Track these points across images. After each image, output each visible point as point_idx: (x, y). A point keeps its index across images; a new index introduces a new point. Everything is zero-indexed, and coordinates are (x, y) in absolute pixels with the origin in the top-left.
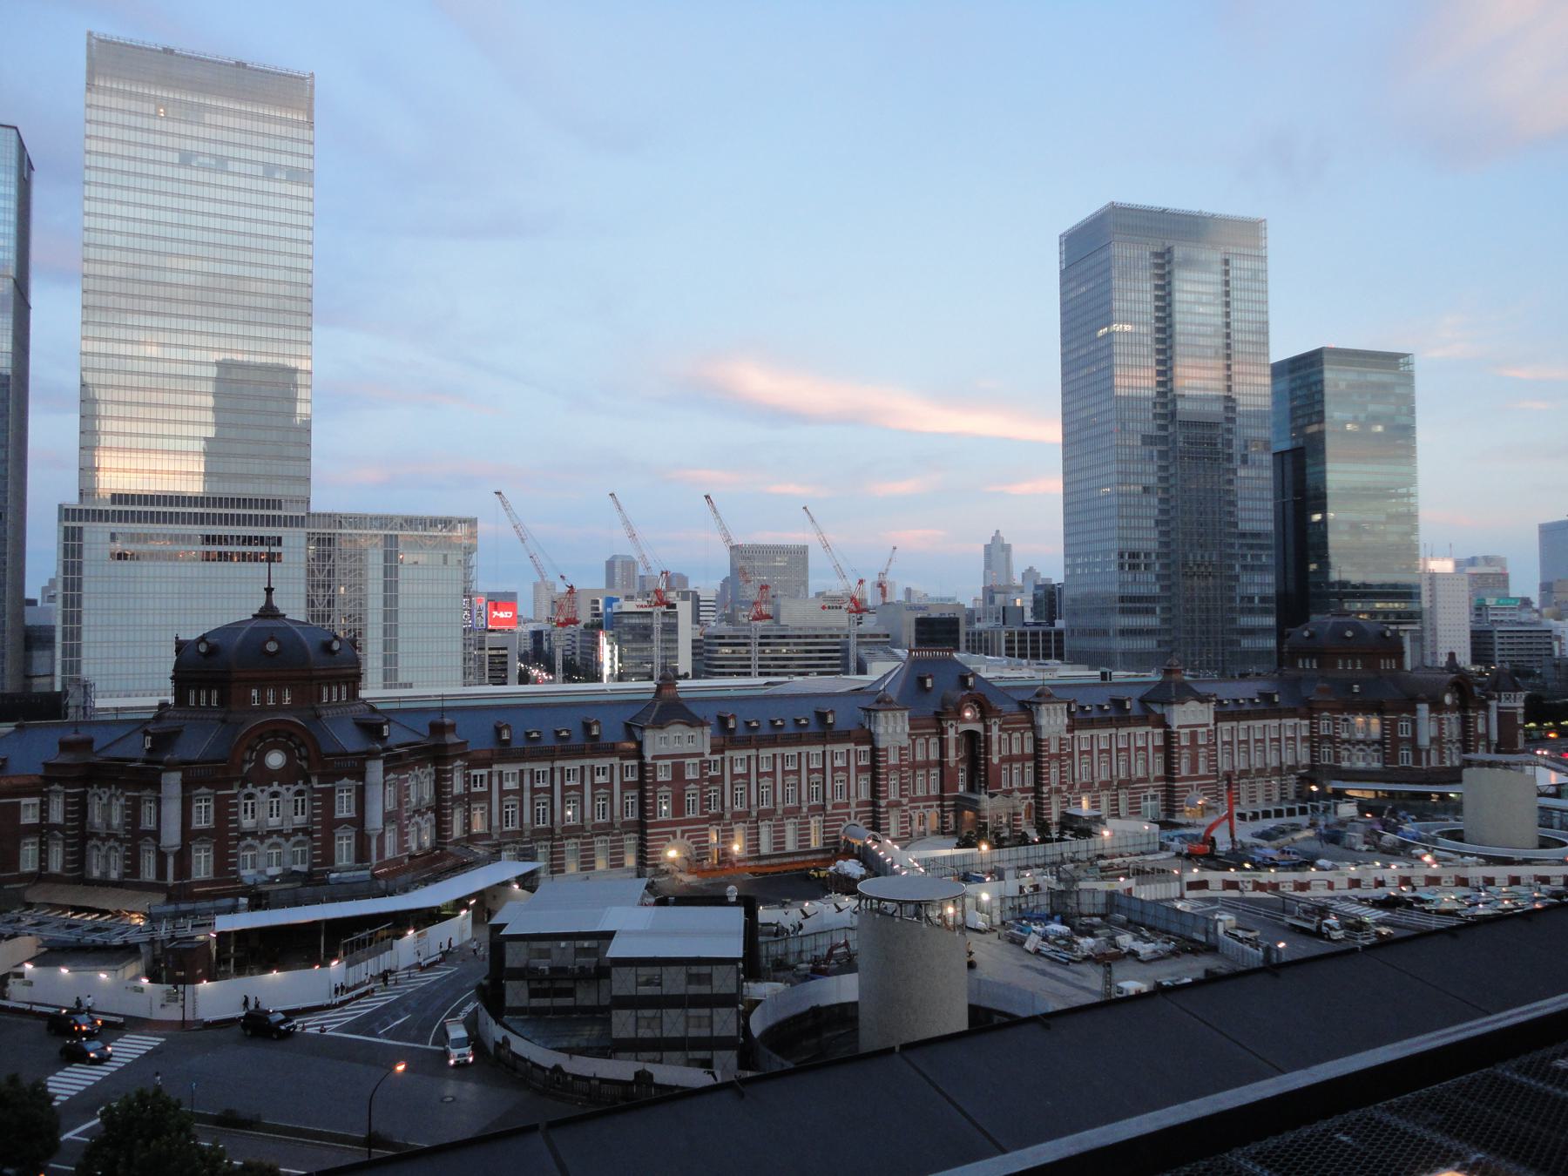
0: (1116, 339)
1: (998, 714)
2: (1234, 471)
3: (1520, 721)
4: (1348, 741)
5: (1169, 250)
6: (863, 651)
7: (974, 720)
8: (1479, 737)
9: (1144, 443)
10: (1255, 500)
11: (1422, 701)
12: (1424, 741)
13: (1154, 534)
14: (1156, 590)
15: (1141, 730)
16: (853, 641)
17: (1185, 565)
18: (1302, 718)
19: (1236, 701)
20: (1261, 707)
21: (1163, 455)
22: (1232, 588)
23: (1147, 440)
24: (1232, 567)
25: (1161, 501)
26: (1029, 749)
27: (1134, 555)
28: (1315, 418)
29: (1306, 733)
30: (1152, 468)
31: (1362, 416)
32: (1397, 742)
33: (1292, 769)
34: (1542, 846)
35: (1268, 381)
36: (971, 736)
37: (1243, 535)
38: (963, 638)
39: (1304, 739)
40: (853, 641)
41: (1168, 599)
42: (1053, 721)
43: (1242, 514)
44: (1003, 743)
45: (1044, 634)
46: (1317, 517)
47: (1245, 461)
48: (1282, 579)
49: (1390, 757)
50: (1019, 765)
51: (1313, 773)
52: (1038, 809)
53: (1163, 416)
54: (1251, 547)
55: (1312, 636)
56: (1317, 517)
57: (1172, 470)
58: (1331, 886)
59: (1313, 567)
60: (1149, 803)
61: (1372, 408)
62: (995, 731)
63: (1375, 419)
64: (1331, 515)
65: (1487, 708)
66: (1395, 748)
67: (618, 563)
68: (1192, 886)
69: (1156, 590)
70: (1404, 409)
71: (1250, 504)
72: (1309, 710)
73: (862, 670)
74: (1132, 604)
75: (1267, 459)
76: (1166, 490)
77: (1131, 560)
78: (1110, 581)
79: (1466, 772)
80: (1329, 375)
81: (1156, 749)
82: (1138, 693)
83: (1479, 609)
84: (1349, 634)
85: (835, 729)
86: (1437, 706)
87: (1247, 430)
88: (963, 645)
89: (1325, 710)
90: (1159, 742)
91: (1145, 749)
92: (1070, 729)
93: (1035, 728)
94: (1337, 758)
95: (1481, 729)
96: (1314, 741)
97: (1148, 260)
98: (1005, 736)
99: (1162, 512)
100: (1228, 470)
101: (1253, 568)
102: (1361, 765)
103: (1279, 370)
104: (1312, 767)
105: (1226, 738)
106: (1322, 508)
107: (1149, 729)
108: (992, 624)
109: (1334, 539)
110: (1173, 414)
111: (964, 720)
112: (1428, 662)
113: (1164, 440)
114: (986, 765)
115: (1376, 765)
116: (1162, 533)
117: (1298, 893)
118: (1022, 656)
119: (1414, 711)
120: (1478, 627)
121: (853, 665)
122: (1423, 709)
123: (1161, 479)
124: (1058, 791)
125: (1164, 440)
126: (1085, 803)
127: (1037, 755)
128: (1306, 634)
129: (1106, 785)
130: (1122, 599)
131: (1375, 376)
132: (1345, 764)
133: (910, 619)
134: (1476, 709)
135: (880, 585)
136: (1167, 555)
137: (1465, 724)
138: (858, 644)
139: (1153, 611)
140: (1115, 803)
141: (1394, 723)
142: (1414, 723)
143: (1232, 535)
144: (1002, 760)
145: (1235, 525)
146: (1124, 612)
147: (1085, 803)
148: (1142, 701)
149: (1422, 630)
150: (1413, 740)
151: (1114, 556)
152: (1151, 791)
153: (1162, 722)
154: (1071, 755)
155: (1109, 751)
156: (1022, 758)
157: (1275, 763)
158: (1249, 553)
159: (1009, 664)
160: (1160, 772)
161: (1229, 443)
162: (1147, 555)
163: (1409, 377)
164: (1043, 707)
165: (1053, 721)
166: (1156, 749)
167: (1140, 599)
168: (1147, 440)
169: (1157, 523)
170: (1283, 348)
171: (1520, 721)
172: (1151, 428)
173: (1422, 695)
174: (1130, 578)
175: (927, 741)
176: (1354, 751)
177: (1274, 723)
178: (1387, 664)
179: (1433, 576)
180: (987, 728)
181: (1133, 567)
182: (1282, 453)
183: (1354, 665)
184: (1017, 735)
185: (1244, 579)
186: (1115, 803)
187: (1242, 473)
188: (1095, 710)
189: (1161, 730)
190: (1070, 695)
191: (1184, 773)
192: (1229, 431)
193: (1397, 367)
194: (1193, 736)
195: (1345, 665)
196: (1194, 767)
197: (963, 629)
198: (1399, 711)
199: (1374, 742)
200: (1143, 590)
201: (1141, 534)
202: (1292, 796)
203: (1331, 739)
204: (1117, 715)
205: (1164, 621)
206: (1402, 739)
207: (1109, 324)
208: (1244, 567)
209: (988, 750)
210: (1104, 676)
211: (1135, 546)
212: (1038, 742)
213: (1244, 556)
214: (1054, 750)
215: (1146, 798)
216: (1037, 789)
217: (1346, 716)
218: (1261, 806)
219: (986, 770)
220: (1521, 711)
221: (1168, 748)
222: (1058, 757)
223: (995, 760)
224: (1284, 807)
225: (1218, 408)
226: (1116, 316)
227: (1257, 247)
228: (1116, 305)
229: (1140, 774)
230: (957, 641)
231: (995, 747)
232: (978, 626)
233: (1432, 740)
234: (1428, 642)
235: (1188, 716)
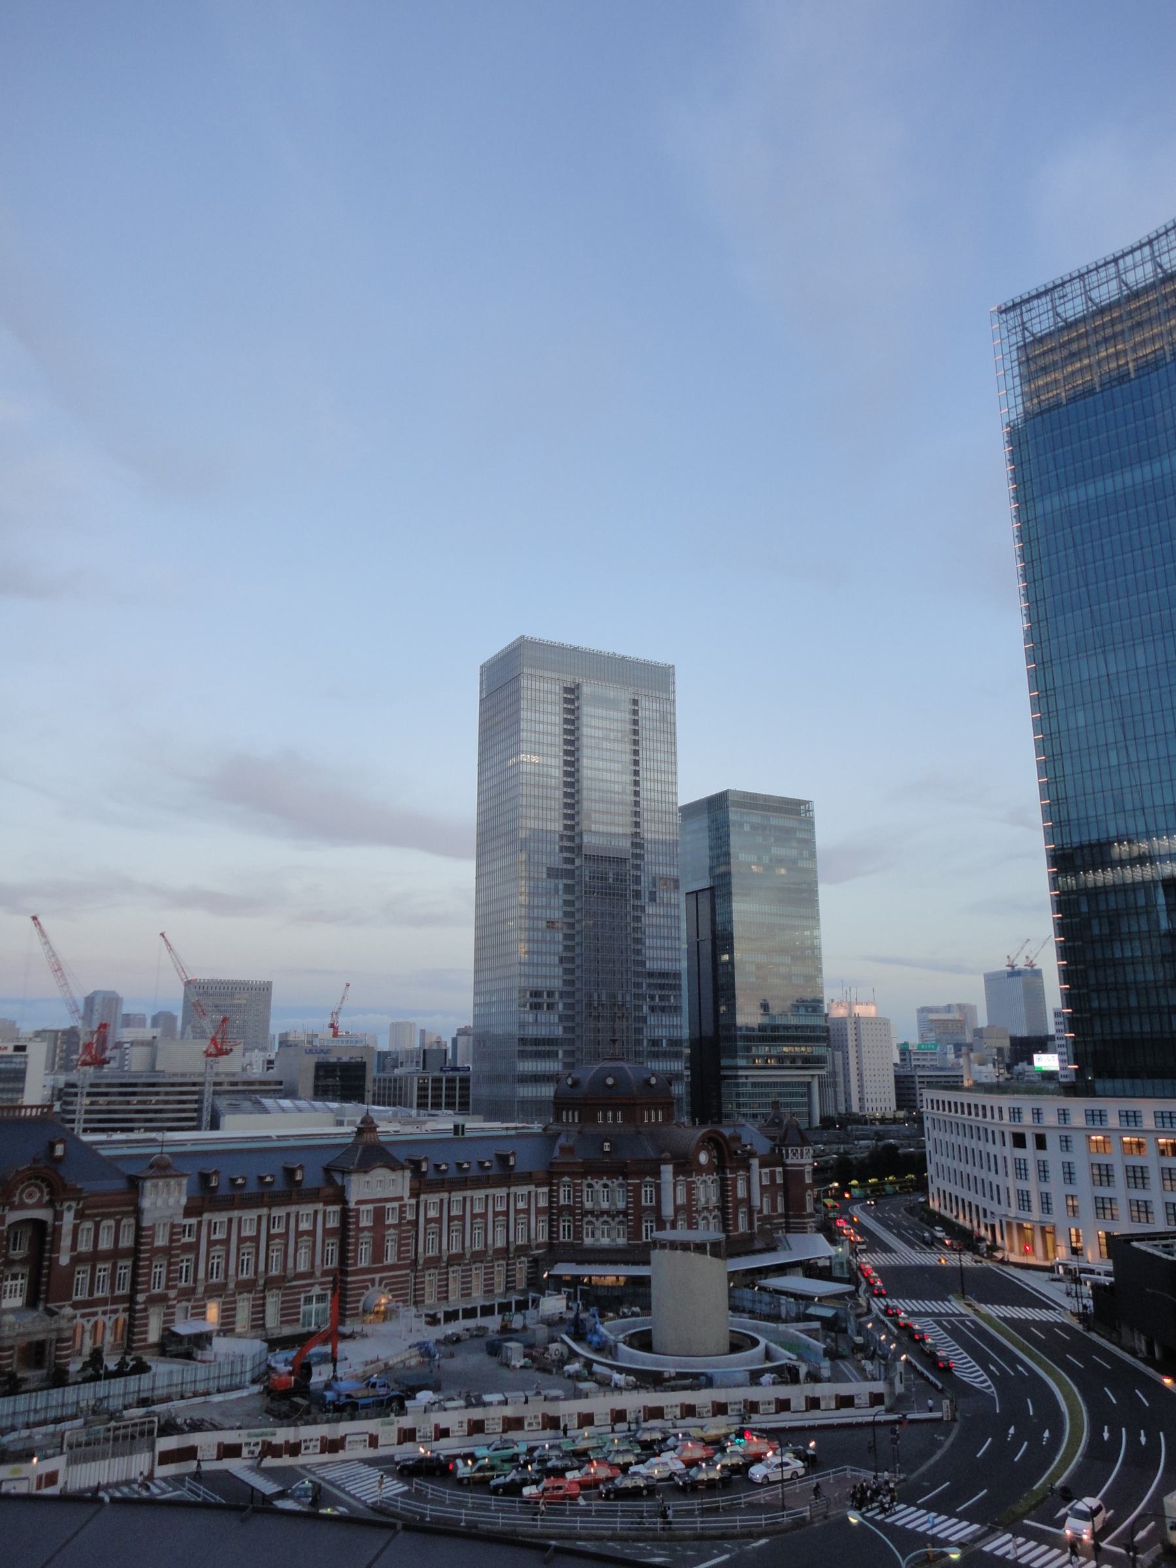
0: (523, 768)
1: (77, 1195)
2: (643, 909)
3: (808, 1180)
4: (592, 1213)
5: (578, 686)
6: (222, 1103)
7: (39, 1205)
8: (738, 1203)
9: (549, 876)
10: (668, 937)
11: (666, 1162)
12: (668, 1211)
13: (559, 971)
14: (559, 1031)
15: (307, 1209)
16: (208, 1089)
17: (589, 1005)
18: (537, 1185)
19: (459, 1165)
20: (491, 1173)
21: (569, 889)
22: (639, 1031)
23: (552, 873)
24: (639, 1008)
25: (567, 937)
26: (127, 1242)
27: (536, 994)
28: (722, 859)
29: (543, 1203)
30: (557, 901)
31: (766, 859)
32: (639, 1211)
33: (522, 1250)
34: (735, 1348)
35: (677, 819)
36: (39, 1226)
37: (651, 975)
38: (369, 1085)
39: (539, 1211)
40: (208, 1089)
41: (571, 1042)
42: (163, 1203)
43: (649, 953)
44: (74, 1236)
45: (461, 1080)
46: (726, 957)
47: (653, 899)
48: (697, 1019)
49: (635, 1233)
50: (108, 1265)
51: (555, 1251)
52: (131, 1330)
53: (570, 850)
54: (662, 987)
55: (576, 1083)
56: (726, 957)
57: (577, 905)
58: (373, 1441)
59: (723, 1009)
60: (314, 1306)
61: (777, 851)
62: (69, 1219)
63: (780, 861)
64: (737, 955)
65: (748, 1168)
66: (638, 1221)
67: (98, 1000)
68: (166, 1458)
69: (559, 1031)
70: (806, 853)
71: (659, 942)
72: (550, 1177)
73: (215, 1125)
74: (538, 1047)
75: (680, 899)
76: (571, 926)
77: (537, 1000)
78: (513, 1020)
79: (656, 1254)
80: (734, 815)
81: (327, 1233)
82: (328, 1158)
83: (904, 1051)
84: (610, 1081)
85: (305, 1186)
86: (685, 1166)
87: (654, 867)
88: (369, 1096)
89: (563, 1174)
90: (333, 1223)
91: (312, 1233)
92: (188, 1212)
93: (138, 1212)
94: (578, 1234)
95: (741, 1193)
96: (553, 1213)
97: (557, 695)
98: (89, 1224)
99: (566, 948)
100: (635, 907)
101: (663, 1009)
102: (605, 1241)
103: (689, 811)
104: (550, 1246)
105: (432, 1214)
106: (731, 952)
107: (320, 1206)
108: (413, 1068)
109: (739, 980)
110: (580, 847)
111: (23, 1206)
112: (855, 1109)
113: (570, 874)
114: (49, 1267)
115: (622, 1241)
116: (566, 971)
117: (326, 1457)
118: (436, 1105)
119: (657, 1174)
120: (902, 1072)
121: (206, 1117)
122: (667, 1170)
123: (566, 914)
124: (163, 1298)
125: (570, 874)
126: (213, 1311)
127: (135, 1252)
128: (570, 1081)
129: (246, 1286)
130: (522, 1041)
131: (777, 821)
132: (588, 1241)
133: (310, 1062)
134: (734, 1170)
135: (332, 1026)
136: (571, 994)
137: (724, 1189)
138: (215, 1093)
139: (552, 1055)
140: (259, 1311)
141: (637, 1189)
142: (658, 1188)
143: (637, 974)
144: (77, 1259)
145: (643, 963)
146: (523, 1055)
147: (213, 1311)
148: (327, 1170)
149: (834, 1074)
150: (658, 1209)
151: (515, 995)
152: (316, 1290)
153: (340, 1197)
154: (194, 1247)
155: (256, 1239)
156: (115, 1254)
157: (500, 1244)
158: (657, 993)
159: (395, 1114)
160: (333, 1264)
161: (637, 880)
162: (550, 994)
163: (810, 823)
164: (148, 1184)
165: (163, 1203)
166: (327, 1233)
167: (537, 1041)
168: (552, 873)
169: (562, 960)
170: (692, 788)
171: (808, 1180)
172: (556, 860)
173: (667, 1155)
174: (531, 1018)
175: (118, 1223)
176: (598, 1224)
177: (501, 1192)
178: (653, 1117)
179: (857, 1020)
180: (58, 1216)
181: (536, 1007)
182: (697, 892)
183: (615, 1118)
184: (112, 1223)
185: (652, 1020)
186: (259, 1311)
187: (650, 910)
188: (475, 1166)
189: (337, 1208)
190: (417, 1154)
191: (363, 1264)
192: (637, 867)
193: (798, 813)
194: (379, 1215)
195: (605, 1118)
196: (378, 1252)
197: (372, 1073)
198: (641, 1174)
199: (619, 1213)
200: (543, 1032)
201: (544, 971)
202: (522, 1286)
203: (570, 1210)
204: (291, 1190)
205: (567, 1065)
206: (647, 1208)
207: (517, 754)
208: (653, 1009)
209: (56, 1248)
210: (456, 1127)
211: (539, 984)
212: (139, 1228)
213: (652, 997)
214: (161, 1241)
215: (308, 1300)
216: (131, 1299)
217: (589, 1181)
218: (478, 1299)
219: (48, 1275)
220: (809, 1169)
221: (344, 1233)
222: (167, 1251)
223: (64, 1260)
224: (514, 1298)
225: (626, 844)
226: (523, 746)
227: (667, 691)
228: (523, 735)
229: (303, 1267)
230: (362, 1088)
231: (66, 1242)
232: (398, 1071)
233: (677, 1209)
234: (841, 1089)
235: (369, 1188)
